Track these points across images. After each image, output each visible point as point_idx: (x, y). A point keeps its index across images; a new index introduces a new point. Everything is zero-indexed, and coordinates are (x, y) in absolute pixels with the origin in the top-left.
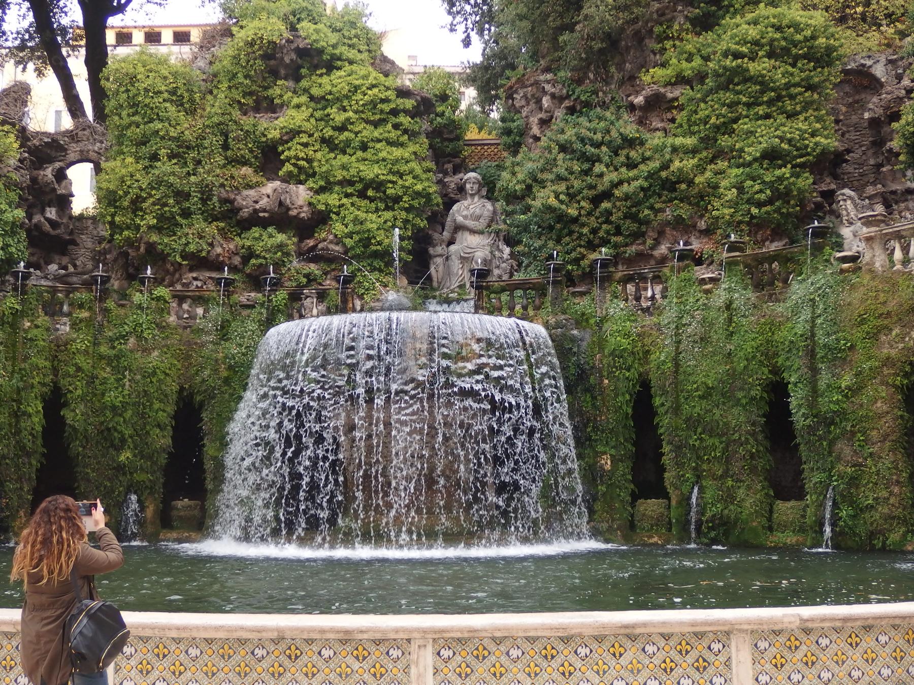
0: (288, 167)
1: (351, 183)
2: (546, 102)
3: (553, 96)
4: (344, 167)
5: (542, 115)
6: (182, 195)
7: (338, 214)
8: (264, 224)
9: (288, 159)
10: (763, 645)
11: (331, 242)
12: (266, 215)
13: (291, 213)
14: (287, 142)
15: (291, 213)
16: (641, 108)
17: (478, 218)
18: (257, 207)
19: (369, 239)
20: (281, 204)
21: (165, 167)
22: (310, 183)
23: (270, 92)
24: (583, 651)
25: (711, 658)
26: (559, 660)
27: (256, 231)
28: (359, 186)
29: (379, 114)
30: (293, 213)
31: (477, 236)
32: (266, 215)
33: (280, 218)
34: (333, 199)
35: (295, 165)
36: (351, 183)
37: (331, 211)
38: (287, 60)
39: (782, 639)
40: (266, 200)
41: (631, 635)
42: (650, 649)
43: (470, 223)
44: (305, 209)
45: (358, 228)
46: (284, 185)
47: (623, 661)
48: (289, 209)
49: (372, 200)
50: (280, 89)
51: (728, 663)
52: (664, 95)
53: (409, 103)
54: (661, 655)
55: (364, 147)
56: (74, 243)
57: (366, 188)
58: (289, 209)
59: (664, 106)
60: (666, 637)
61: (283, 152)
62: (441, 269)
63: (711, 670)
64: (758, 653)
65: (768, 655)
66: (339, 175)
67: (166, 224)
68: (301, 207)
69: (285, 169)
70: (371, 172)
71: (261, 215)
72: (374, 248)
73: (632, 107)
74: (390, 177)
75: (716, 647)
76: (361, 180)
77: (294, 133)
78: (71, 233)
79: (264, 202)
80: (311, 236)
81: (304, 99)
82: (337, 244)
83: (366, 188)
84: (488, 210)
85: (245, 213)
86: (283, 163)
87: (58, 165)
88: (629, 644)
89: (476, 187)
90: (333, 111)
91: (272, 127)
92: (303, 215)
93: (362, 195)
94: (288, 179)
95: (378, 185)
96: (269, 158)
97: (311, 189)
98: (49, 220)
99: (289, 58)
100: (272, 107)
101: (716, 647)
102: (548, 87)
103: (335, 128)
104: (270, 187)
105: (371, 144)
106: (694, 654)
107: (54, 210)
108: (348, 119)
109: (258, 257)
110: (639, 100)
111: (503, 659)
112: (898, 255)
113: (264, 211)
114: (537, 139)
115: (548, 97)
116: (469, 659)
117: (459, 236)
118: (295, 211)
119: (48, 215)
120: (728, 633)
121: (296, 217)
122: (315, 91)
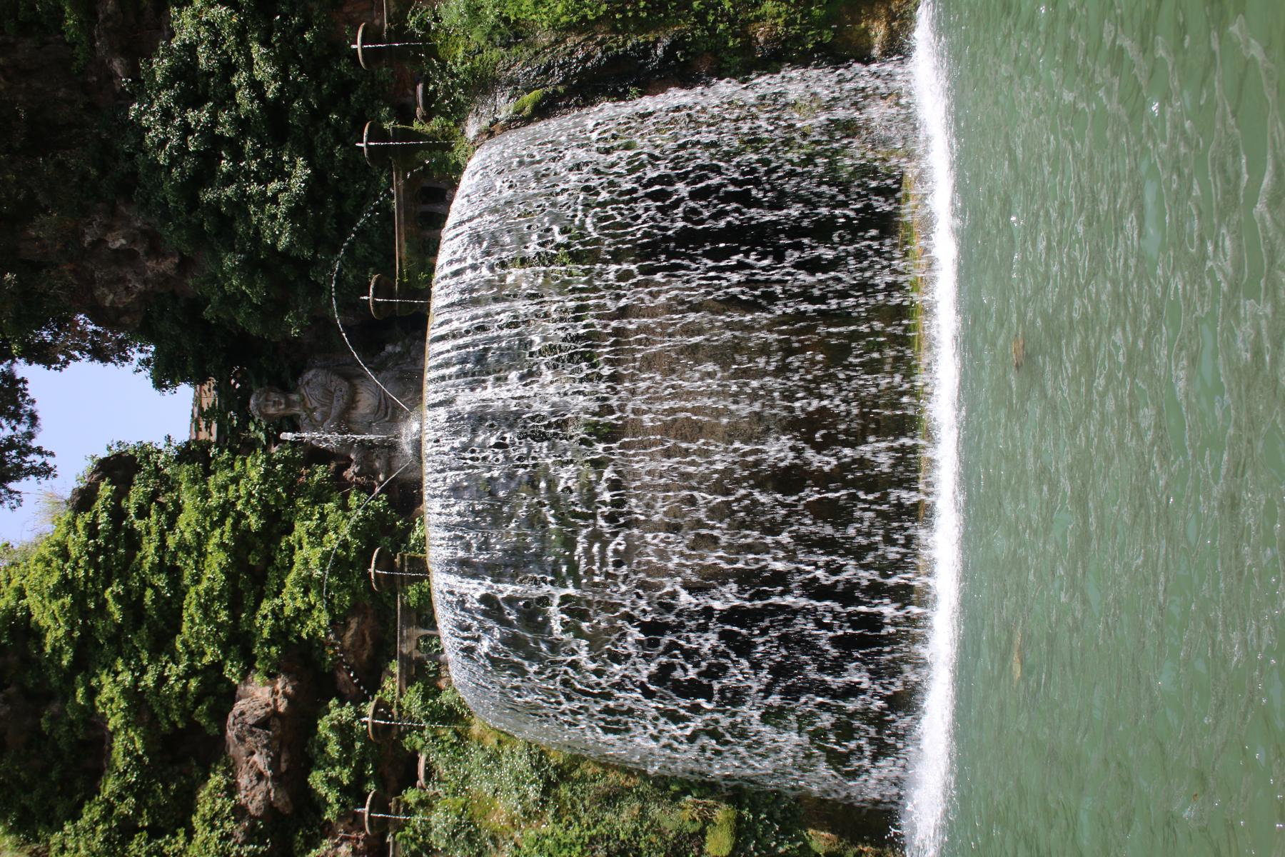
0: (201, 714)
5: (140, 249)
9: (187, 715)
12: (283, 758)
13: (281, 709)
15: (281, 709)
17: (329, 394)
20: (263, 723)
23: (62, 744)
27: (316, 779)
30: (282, 706)
31: (359, 397)
35: (199, 700)
40: (256, 757)
43: (337, 406)
48: (275, 712)
53: (105, 490)
58: (275, 712)
61: (174, 724)
68: (275, 692)
69: (203, 721)
71: (284, 766)
74: (229, 521)
80: (332, 676)
82: (346, 626)
84: (315, 376)
86: (193, 726)
89: (274, 397)
92: (289, 689)
95: (242, 543)
97: (244, 676)
103: (136, 629)
108: (117, 598)
114: (185, 264)
115: (109, 237)
118: (279, 702)
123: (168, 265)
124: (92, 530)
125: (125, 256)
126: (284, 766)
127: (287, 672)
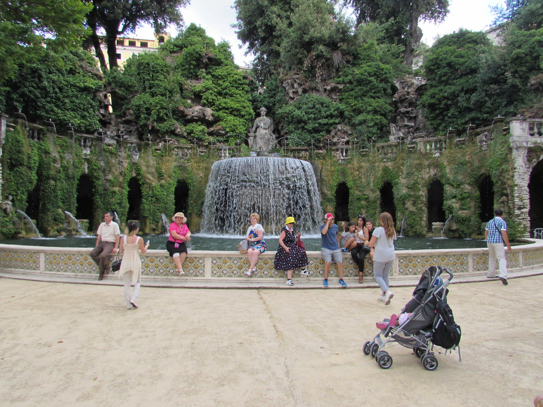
1: (227, 109)
2: (296, 86)
3: (299, 84)
4: (225, 103)
5: (294, 90)
8: (196, 121)
10: (475, 258)
14: (204, 92)
16: (329, 91)
20: (204, 114)
22: (213, 108)
24: (435, 260)
25: (464, 261)
26: (429, 262)
29: (237, 84)
30: (207, 118)
33: (202, 120)
34: (221, 113)
36: (227, 109)
38: (204, 61)
39: (478, 256)
41: (446, 255)
42: (451, 259)
44: (211, 117)
46: (203, 108)
47: (444, 262)
49: (235, 115)
50: (202, 72)
51: (467, 263)
52: (337, 87)
54: (453, 260)
55: (231, 96)
56: (110, 123)
57: (233, 111)
58: (205, 116)
59: (337, 91)
60: (454, 256)
62: (252, 141)
63: (464, 264)
64: (474, 260)
65: (476, 261)
66: (224, 105)
67: (160, 120)
70: (236, 105)
73: (325, 90)
75: (465, 258)
76: (231, 108)
77: (207, 89)
78: (110, 119)
79: (196, 113)
81: (209, 76)
83: (233, 111)
85: (189, 117)
87: (105, 93)
88: (446, 258)
89: (265, 113)
90: (220, 82)
91: (198, 86)
93: (231, 113)
94: (204, 105)
95: (238, 110)
96: (197, 97)
98: (102, 114)
99: (205, 60)
100: (196, 77)
101: (465, 258)
102: (297, 81)
104: (198, 108)
106: (460, 260)
107: (103, 110)
109: (194, 133)
110: (329, 88)
111: (416, 262)
112: (428, 147)
113: (196, 117)
116: (408, 262)
117: (258, 129)
119: (101, 112)
120: (467, 255)
121: (207, 120)
122: (215, 73)
123: (291, 95)
124: (239, 80)
125: (293, 87)
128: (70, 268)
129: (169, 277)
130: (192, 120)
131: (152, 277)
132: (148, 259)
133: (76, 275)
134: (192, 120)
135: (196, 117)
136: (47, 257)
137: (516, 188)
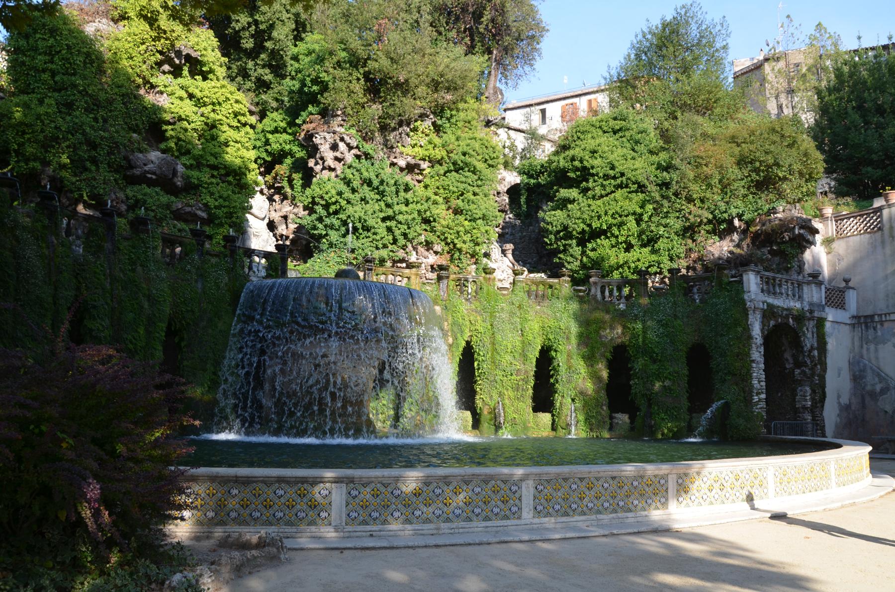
6: (93, 146)
7: (206, 188)
8: (151, 183)
11: (200, 209)
12: (154, 177)
18: (146, 168)
19: (231, 213)
21: (80, 116)
28: (223, 172)
32: (154, 177)
33: (164, 181)
37: (201, 186)
45: (227, 203)
49: (230, 183)
57: (227, 174)
66: (212, 161)
71: (149, 176)
72: (234, 219)
85: (137, 172)
105: (232, 143)
113: (154, 173)
126: (149, 176)
127: (185, 184)
128: (418, 513)
129: (619, 515)
130: (141, 180)
131: (593, 517)
132: (584, 483)
133: (438, 529)
134: (141, 180)
135: (154, 173)
136: (354, 493)
137: (754, 365)
